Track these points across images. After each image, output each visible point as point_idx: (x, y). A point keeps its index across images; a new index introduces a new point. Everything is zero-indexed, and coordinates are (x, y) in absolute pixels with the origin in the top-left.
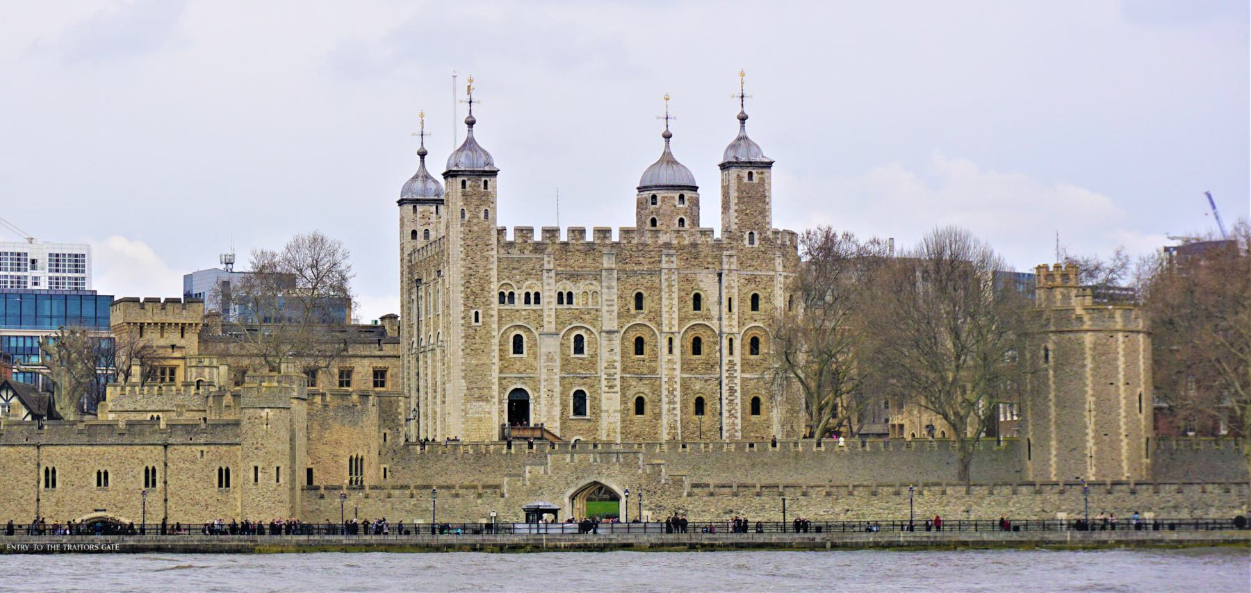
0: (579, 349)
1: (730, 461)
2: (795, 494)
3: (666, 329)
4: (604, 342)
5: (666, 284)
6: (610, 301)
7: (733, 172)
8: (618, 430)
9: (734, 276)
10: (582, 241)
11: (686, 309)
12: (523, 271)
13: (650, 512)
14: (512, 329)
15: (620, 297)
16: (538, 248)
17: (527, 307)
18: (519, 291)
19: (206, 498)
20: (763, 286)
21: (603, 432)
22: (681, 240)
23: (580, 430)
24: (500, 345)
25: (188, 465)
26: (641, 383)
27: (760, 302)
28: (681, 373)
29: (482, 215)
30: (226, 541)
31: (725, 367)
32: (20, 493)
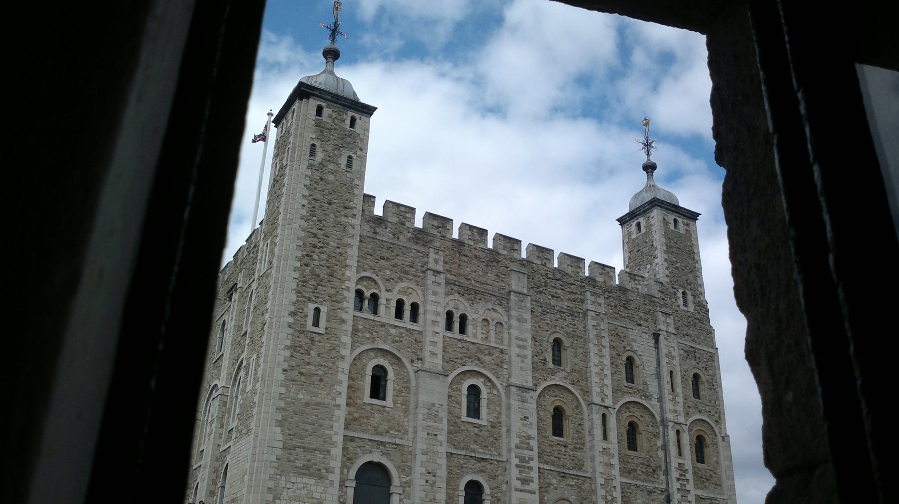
3: (597, 399)
4: (515, 403)
6: (522, 340)
7: (656, 214)
9: (674, 342)
10: (481, 245)
11: (617, 377)
14: (372, 354)
15: (534, 339)
17: (398, 323)
22: (606, 278)
24: (351, 378)
27: (701, 387)
28: (621, 475)
29: (343, 161)
31: (675, 474)
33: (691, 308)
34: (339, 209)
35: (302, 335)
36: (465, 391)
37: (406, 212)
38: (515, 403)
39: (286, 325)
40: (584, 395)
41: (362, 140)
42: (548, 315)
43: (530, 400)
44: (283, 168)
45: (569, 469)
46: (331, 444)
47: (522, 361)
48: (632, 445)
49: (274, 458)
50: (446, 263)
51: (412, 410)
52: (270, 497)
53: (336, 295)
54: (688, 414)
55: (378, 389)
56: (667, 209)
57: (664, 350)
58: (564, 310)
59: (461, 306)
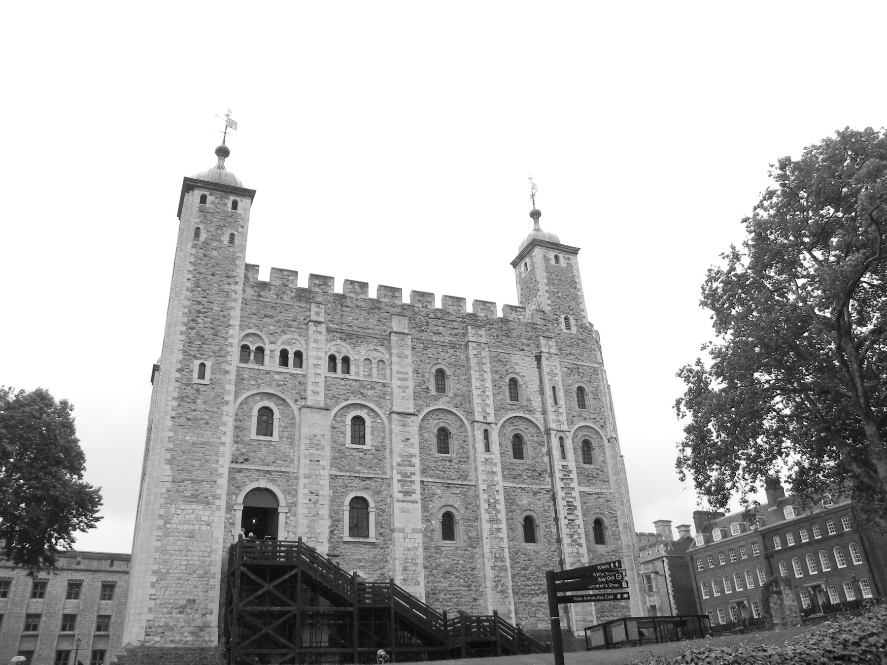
0: (359, 437)
3: (478, 417)
4: (396, 428)
5: (476, 360)
7: (538, 252)
8: (420, 561)
9: (556, 361)
10: (362, 296)
11: (501, 397)
14: (258, 398)
15: (416, 372)
16: (303, 295)
18: (272, 347)
21: (397, 563)
23: (359, 560)
24: (236, 420)
26: (448, 493)
29: (226, 239)
31: (558, 475)
33: (574, 330)
34: (222, 279)
35: (189, 387)
37: (289, 276)
38: (396, 428)
39: (173, 380)
40: (468, 415)
41: (243, 219)
42: (430, 350)
43: (411, 424)
45: (454, 480)
46: (217, 475)
47: (404, 392)
48: (518, 453)
49: (164, 491)
50: (328, 314)
51: (296, 442)
52: (161, 522)
53: (220, 351)
54: (572, 422)
56: (547, 247)
58: (446, 344)
59: (343, 349)
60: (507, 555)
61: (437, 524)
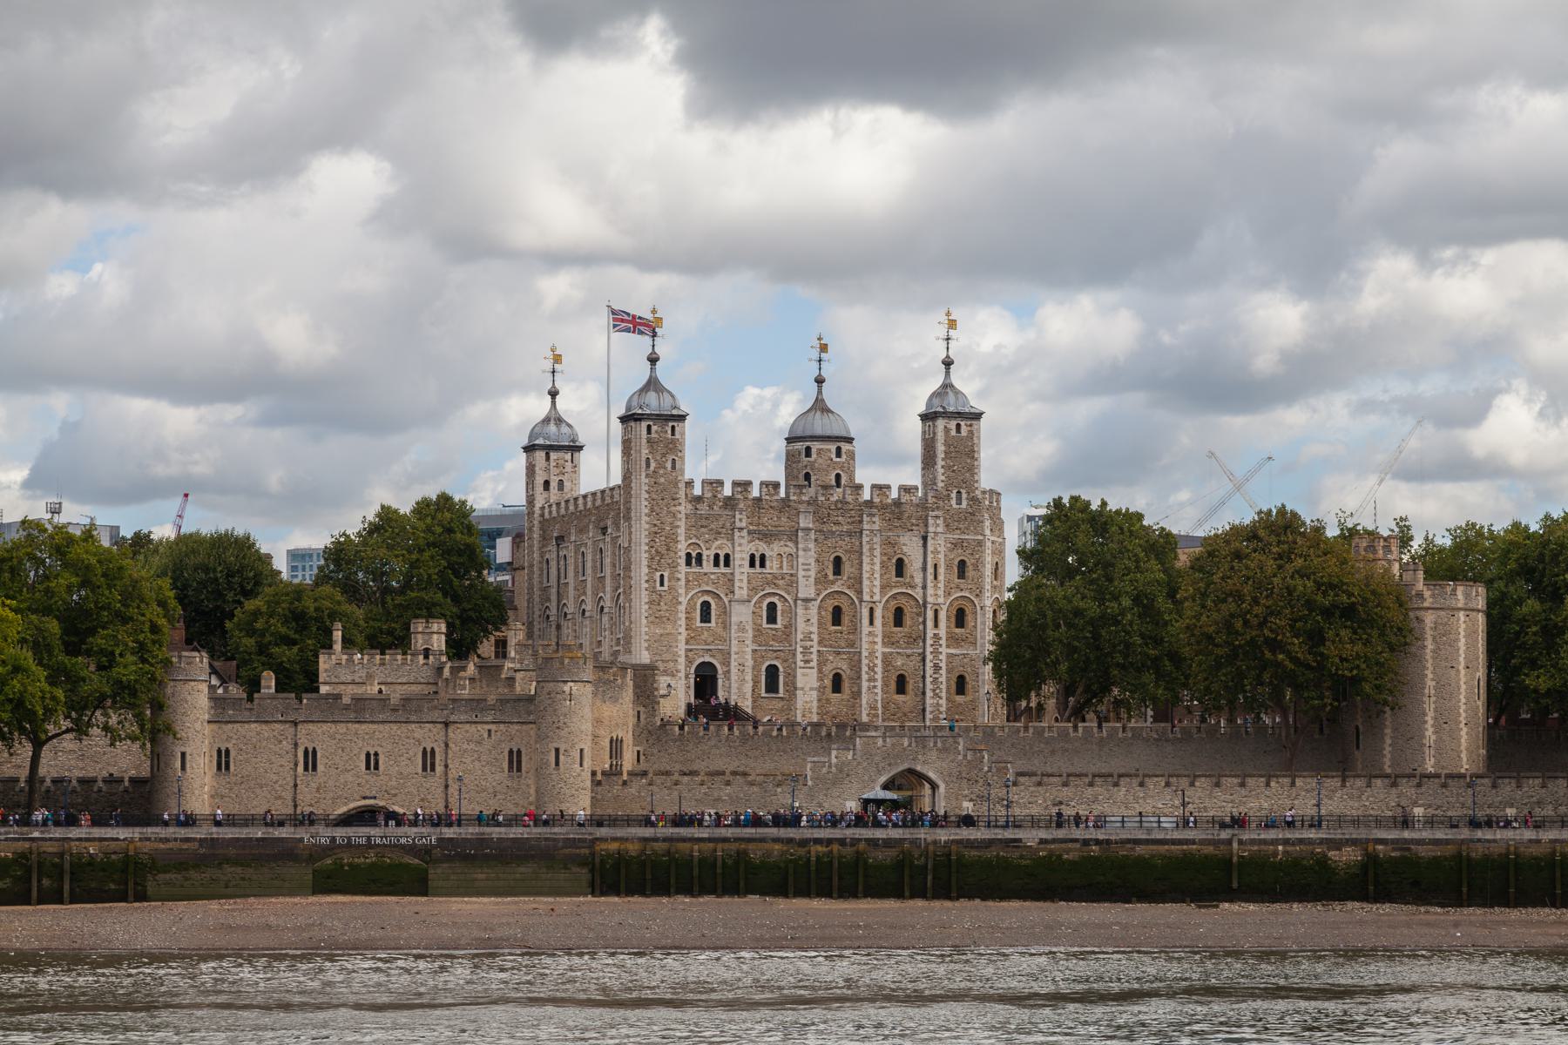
0: (772, 618)
1: (1027, 747)
2: (1131, 784)
3: (866, 597)
5: (868, 547)
7: (941, 423)
8: (815, 710)
10: (776, 497)
12: (712, 530)
13: (972, 804)
15: (817, 561)
16: (730, 503)
17: (716, 570)
19: (494, 784)
20: (970, 551)
21: (798, 712)
23: (772, 709)
25: (472, 746)
29: (669, 465)
30: (560, 833)
31: (929, 642)
32: (275, 778)
33: (964, 503)
36: (765, 608)
38: (800, 611)
44: (628, 469)
55: (706, 617)
57: (930, 548)
59: (760, 547)
60: (879, 705)
61: (828, 682)
